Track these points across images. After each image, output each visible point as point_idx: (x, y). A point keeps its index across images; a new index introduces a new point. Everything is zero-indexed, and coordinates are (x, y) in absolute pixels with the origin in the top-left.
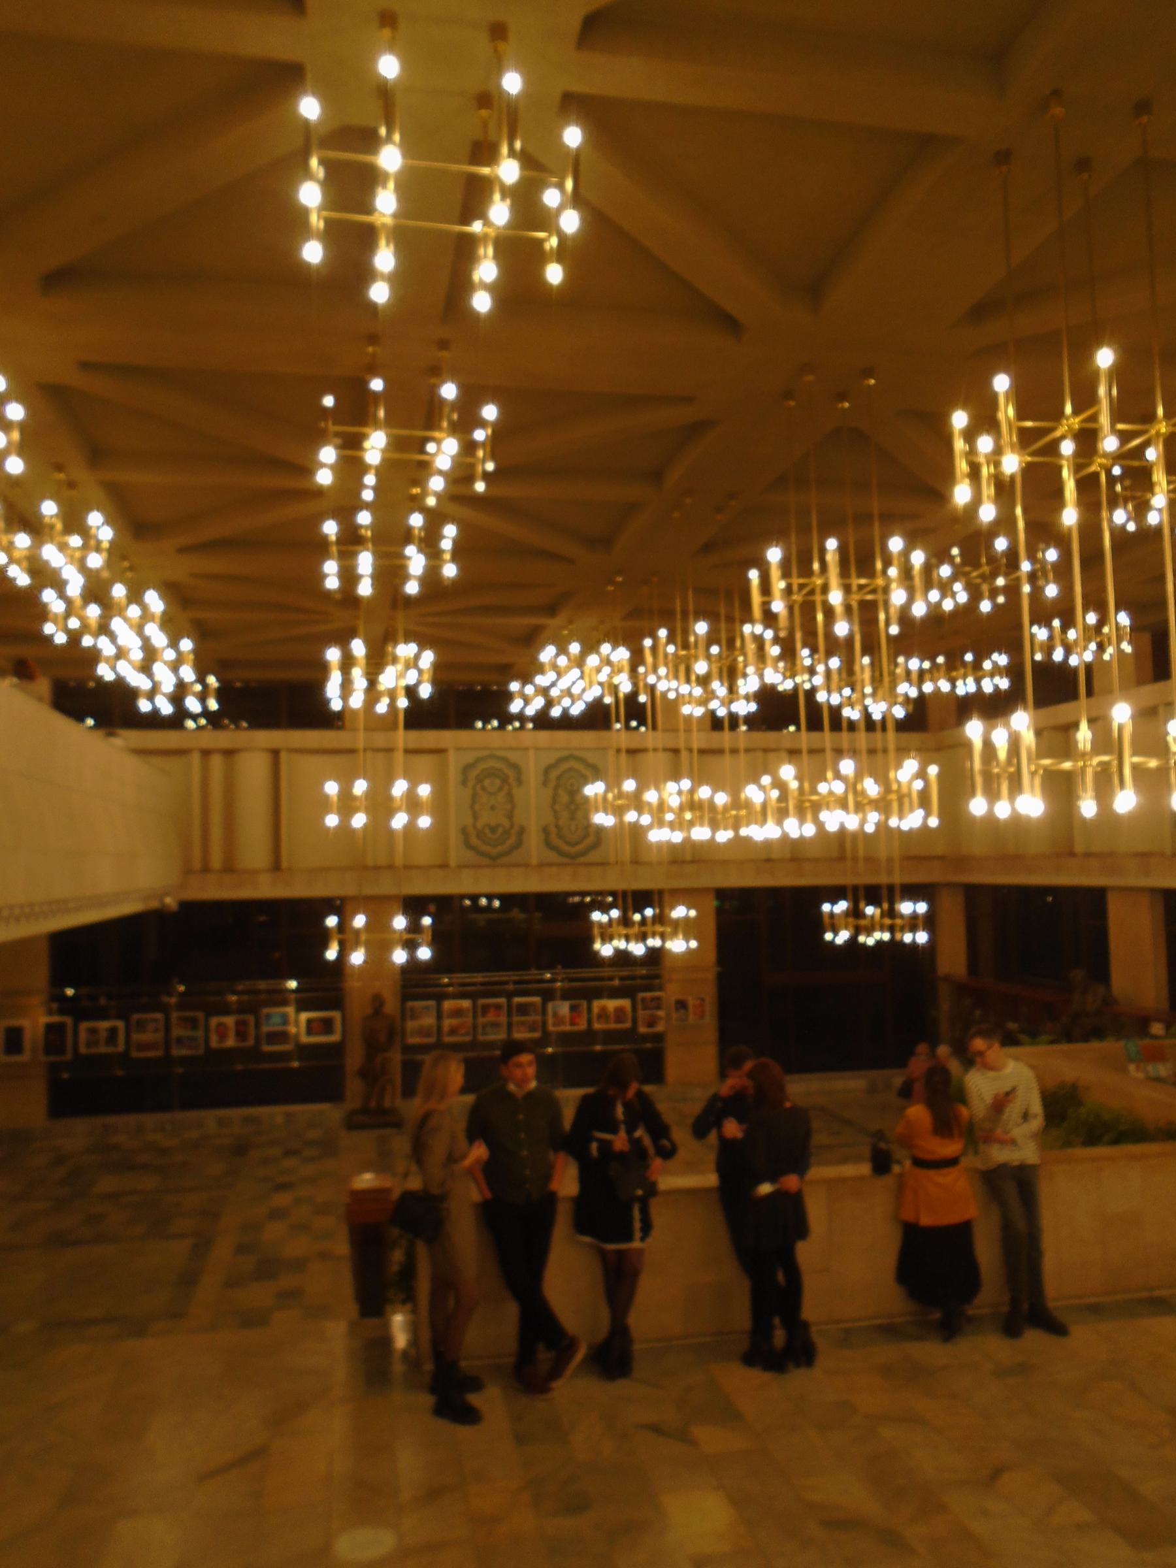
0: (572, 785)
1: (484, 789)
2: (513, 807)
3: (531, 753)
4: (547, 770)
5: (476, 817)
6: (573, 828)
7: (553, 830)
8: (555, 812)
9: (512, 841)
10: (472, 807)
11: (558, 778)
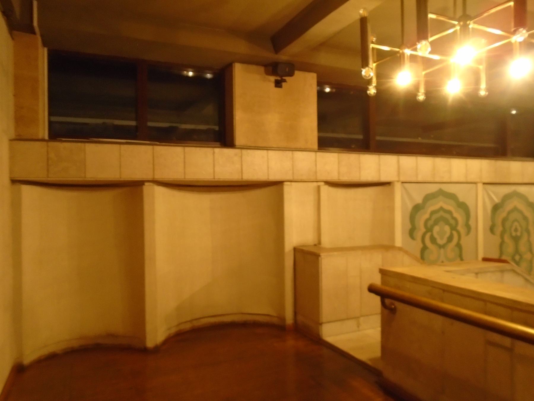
0: (516, 230)
1: (433, 240)
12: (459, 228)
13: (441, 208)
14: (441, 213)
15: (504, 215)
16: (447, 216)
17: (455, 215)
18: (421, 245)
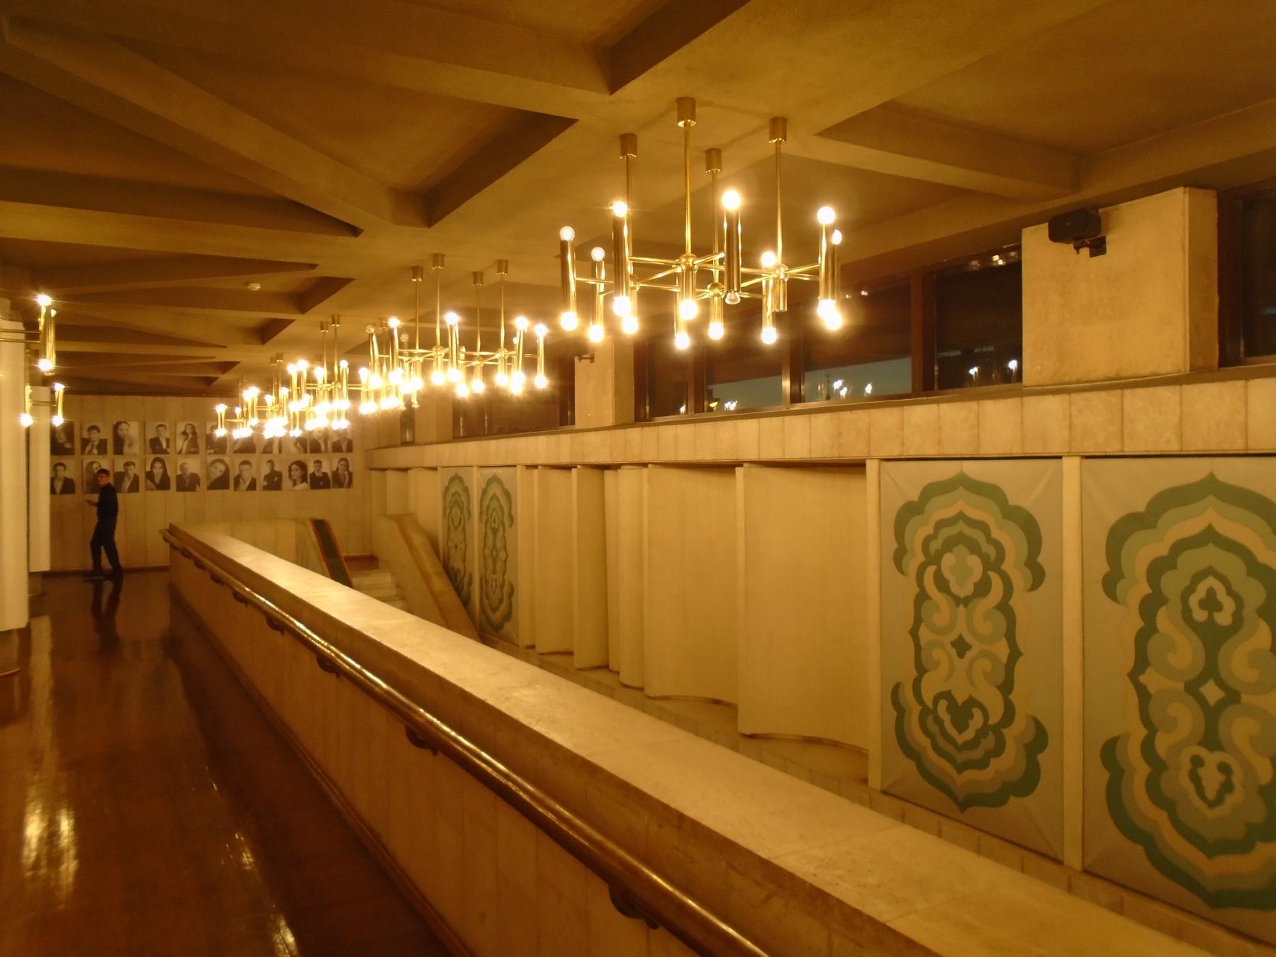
0: (1210, 603)
1: (942, 584)
2: (1015, 654)
3: (1071, 466)
4: (1118, 536)
5: (921, 670)
6: (1211, 779)
7: (1140, 770)
8: (1143, 695)
9: (1008, 762)
10: (914, 633)
11: (1157, 569)
12: (1007, 566)
13: (961, 516)
14: (961, 526)
15: (1162, 549)
16: (978, 535)
17: (996, 534)
18: (917, 590)
